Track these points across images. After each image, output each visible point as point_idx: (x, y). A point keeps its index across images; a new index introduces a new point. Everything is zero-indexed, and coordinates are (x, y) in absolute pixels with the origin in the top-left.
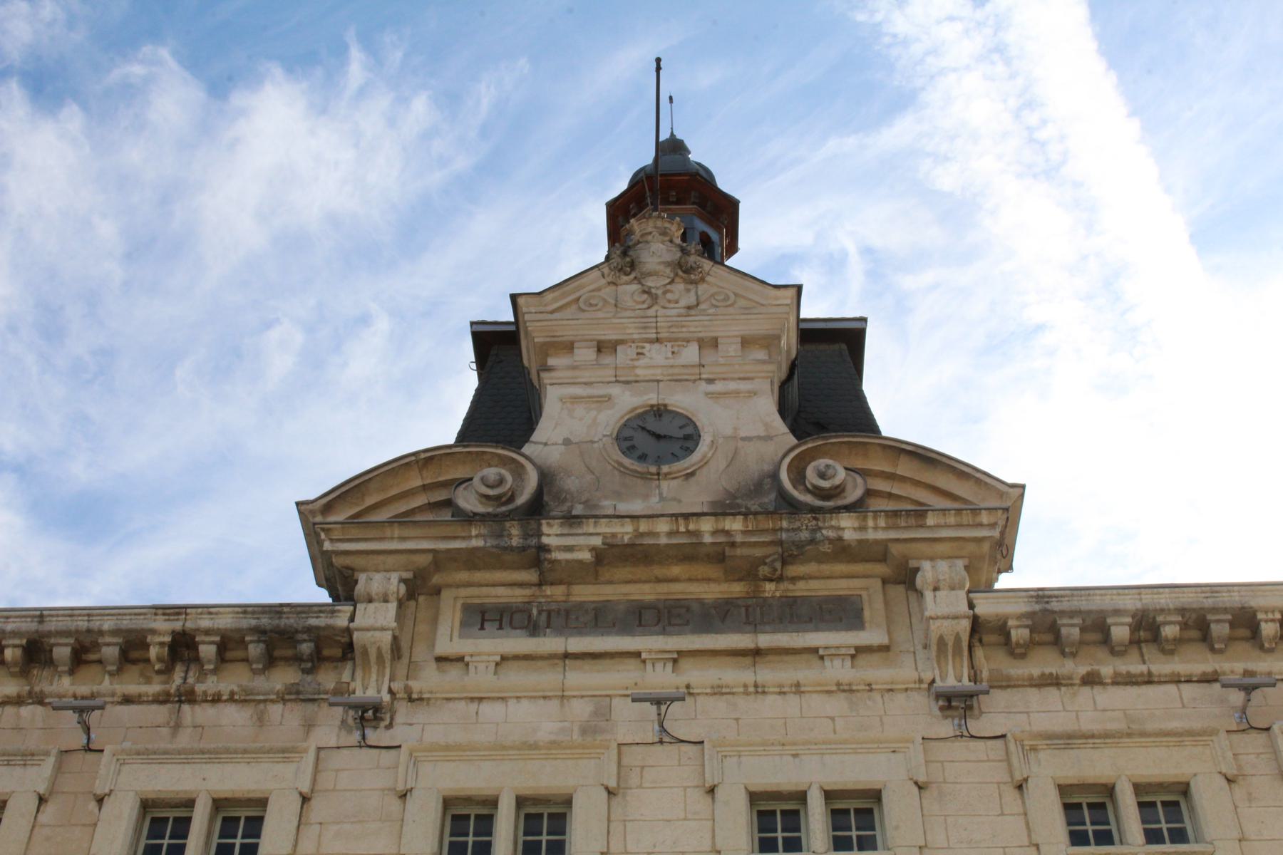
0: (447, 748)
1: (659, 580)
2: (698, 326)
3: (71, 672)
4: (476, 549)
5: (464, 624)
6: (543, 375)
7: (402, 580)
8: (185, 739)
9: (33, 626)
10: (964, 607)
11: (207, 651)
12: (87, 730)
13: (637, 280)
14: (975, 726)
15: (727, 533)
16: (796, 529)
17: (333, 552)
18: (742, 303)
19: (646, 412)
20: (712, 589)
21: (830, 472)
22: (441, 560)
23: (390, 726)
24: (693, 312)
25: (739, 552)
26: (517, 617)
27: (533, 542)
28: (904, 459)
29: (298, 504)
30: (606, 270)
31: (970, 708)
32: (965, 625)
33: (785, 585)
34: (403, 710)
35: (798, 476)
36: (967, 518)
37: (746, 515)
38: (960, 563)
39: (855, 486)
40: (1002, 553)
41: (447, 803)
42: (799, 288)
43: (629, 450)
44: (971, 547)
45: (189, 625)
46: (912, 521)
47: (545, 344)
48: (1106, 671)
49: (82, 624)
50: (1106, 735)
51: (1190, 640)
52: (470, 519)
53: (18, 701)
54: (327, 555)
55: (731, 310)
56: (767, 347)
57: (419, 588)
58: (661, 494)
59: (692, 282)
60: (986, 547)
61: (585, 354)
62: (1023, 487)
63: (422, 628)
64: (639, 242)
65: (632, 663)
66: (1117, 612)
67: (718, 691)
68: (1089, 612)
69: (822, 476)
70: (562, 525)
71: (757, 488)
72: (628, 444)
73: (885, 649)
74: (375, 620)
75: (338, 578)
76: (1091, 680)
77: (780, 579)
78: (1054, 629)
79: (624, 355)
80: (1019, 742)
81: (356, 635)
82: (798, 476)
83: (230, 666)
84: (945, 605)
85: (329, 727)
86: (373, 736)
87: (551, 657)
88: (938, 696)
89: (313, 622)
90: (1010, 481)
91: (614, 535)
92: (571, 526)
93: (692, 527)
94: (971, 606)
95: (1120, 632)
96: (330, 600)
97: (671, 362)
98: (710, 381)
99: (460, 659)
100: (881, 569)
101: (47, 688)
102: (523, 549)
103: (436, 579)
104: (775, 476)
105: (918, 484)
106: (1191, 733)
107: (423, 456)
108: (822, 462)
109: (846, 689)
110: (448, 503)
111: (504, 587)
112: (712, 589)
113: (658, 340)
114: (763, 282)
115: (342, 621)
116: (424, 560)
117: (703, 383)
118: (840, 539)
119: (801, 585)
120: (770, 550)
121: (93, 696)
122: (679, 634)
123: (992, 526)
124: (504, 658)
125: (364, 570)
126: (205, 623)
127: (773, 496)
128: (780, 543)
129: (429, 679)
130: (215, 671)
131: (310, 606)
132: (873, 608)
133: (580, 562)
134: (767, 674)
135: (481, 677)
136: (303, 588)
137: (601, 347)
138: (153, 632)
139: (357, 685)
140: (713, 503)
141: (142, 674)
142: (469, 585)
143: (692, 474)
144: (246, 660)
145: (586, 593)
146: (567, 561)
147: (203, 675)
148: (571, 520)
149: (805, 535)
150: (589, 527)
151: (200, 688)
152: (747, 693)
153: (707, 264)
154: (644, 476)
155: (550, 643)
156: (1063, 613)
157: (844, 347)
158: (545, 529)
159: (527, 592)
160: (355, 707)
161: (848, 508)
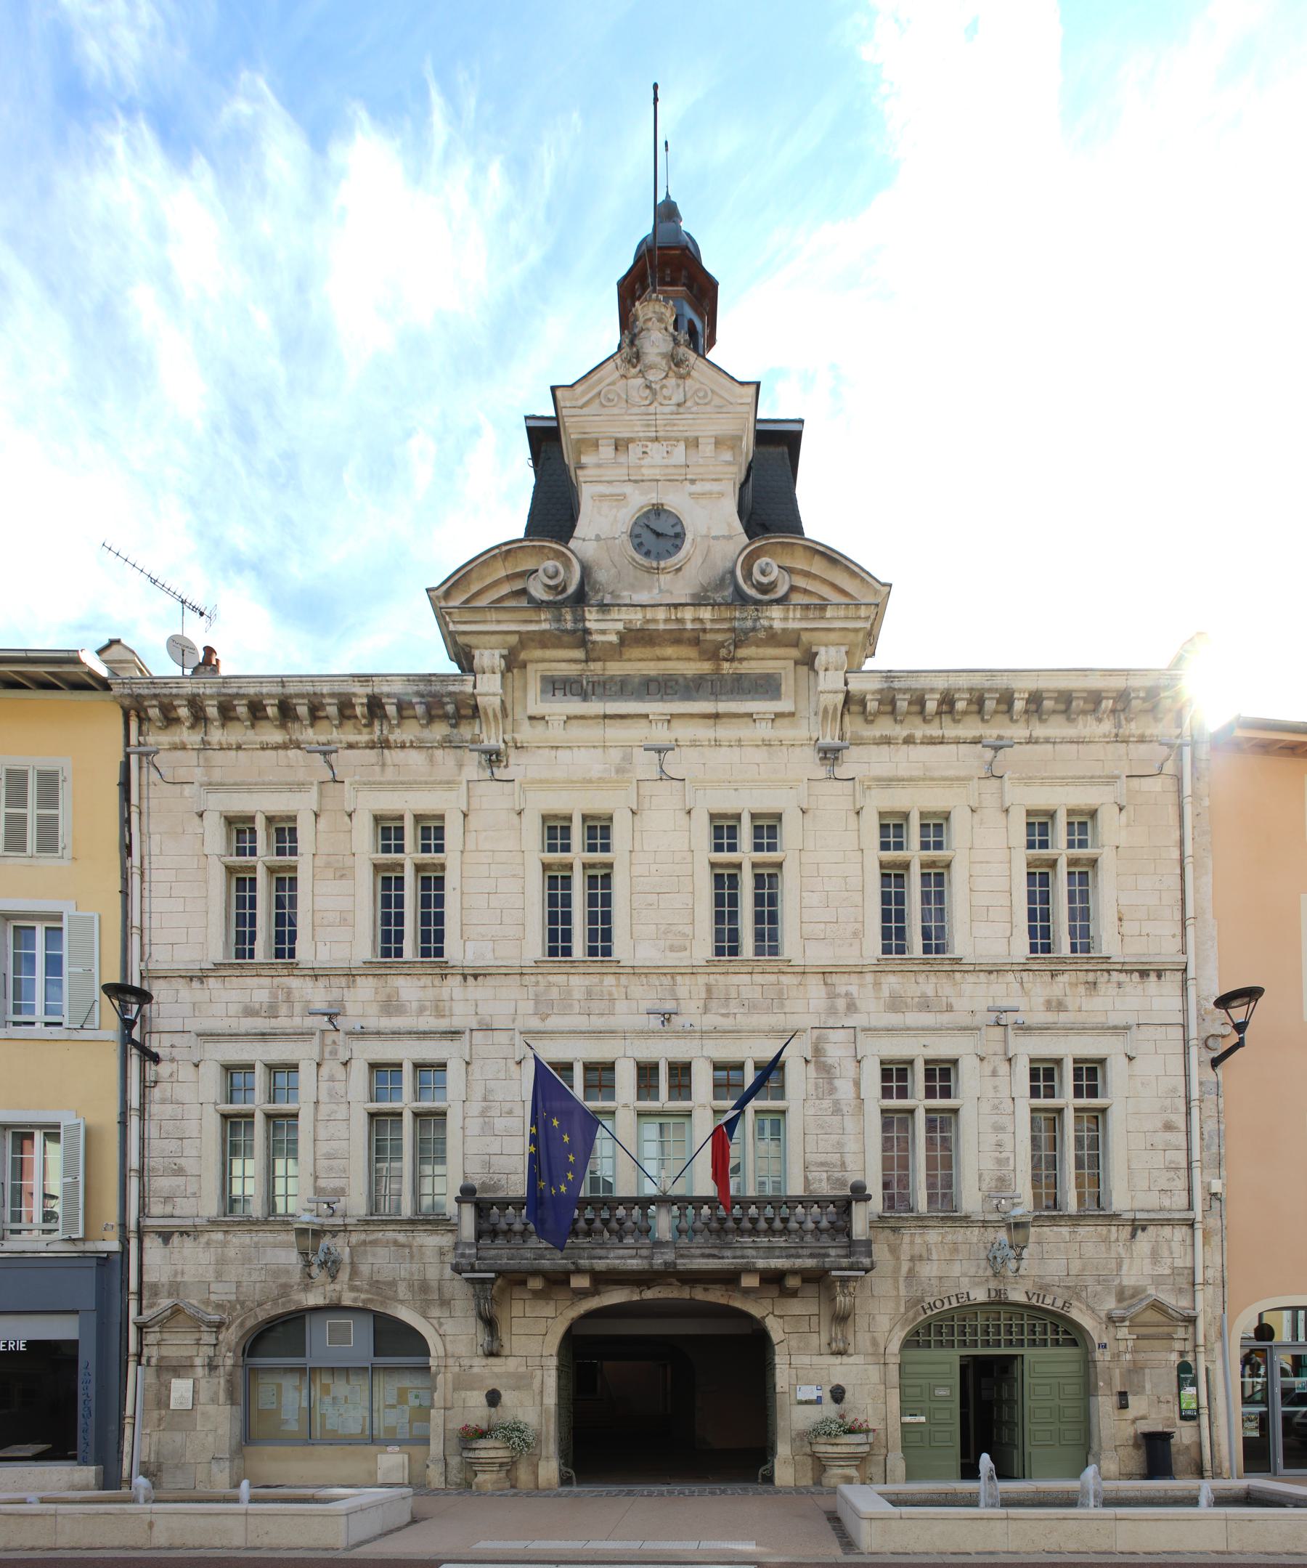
0: (541, 781)
1: (659, 659)
2: (686, 426)
3: (312, 725)
4: (544, 632)
5: (543, 691)
6: (580, 472)
7: (503, 657)
8: (390, 774)
9: (279, 690)
11: (391, 710)
12: (331, 767)
14: (840, 772)
15: (701, 620)
16: (743, 618)
17: (456, 632)
18: (717, 401)
19: (649, 511)
20: (690, 666)
21: (768, 570)
22: (526, 640)
23: (506, 766)
24: (681, 410)
25: (709, 637)
26: (574, 686)
27: (580, 626)
28: (817, 558)
29: (428, 590)
30: (619, 361)
31: (836, 758)
32: (841, 697)
33: (736, 664)
35: (748, 575)
36: (851, 612)
37: (713, 605)
38: (843, 649)
40: (869, 640)
41: (545, 818)
42: (758, 384)
43: (638, 547)
44: (851, 636)
45: (377, 690)
46: (817, 614)
47: (579, 441)
48: (918, 734)
49: (310, 689)
50: (910, 779)
51: (972, 713)
52: (539, 605)
53: (284, 746)
54: (451, 633)
55: (708, 408)
56: (733, 448)
57: (513, 663)
59: (682, 377)
60: (861, 635)
61: (607, 451)
62: (890, 585)
63: (518, 694)
64: (642, 330)
65: (644, 722)
66: (932, 690)
67: (694, 744)
68: (916, 689)
69: (763, 573)
70: (598, 612)
71: (720, 584)
72: (639, 540)
73: (792, 714)
74: (488, 687)
75: (463, 655)
76: (909, 741)
77: (732, 660)
78: (893, 702)
79: (635, 450)
80: (861, 782)
81: (479, 699)
82: (748, 575)
83: (407, 722)
84: (830, 683)
85: (472, 767)
86: (499, 773)
87: (597, 717)
88: (820, 750)
89: (451, 688)
90: (882, 581)
91: (631, 621)
92: (603, 612)
93: (679, 616)
94: (846, 684)
95: (931, 706)
96: (459, 672)
97: (666, 462)
98: (693, 481)
99: (543, 718)
100: (795, 653)
101: (301, 738)
102: (574, 631)
103: (523, 656)
104: (732, 572)
105: (824, 581)
106: (958, 779)
107: (504, 548)
108: (763, 560)
109: (767, 744)
110: (524, 592)
111: (564, 662)
112: (690, 666)
113: (656, 439)
114: (732, 378)
115: (469, 689)
116: (514, 640)
117: (687, 483)
118: (771, 627)
119: (745, 664)
120: (728, 635)
121: (329, 743)
123: (867, 618)
124: (568, 718)
125: (477, 648)
126: (386, 689)
127: (731, 589)
128: (733, 630)
129: (526, 733)
130: (399, 725)
131: (448, 676)
132: (787, 686)
133: (610, 643)
134: (726, 732)
135: (556, 732)
136: (441, 663)
137: (620, 445)
138: (355, 695)
139: (484, 736)
140: (693, 596)
141: (355, 728)
142: (543, 661)
143: (679, 570)
144: (415, 717)
145: (615, 668)
146: (603, 642)
147: (391, 727)
148: (604, 607)
149: (749, 624)
150: (614, 614)
151: (392, 738)
152: (710, 746)
153: (692, 356)
154: (649, 570)
155: (595, 707)
156: (900, 689)
157: (786, 449)
158: (588, 616)
159: (579, 667)
160: (485, 752)
161: (778, 601)
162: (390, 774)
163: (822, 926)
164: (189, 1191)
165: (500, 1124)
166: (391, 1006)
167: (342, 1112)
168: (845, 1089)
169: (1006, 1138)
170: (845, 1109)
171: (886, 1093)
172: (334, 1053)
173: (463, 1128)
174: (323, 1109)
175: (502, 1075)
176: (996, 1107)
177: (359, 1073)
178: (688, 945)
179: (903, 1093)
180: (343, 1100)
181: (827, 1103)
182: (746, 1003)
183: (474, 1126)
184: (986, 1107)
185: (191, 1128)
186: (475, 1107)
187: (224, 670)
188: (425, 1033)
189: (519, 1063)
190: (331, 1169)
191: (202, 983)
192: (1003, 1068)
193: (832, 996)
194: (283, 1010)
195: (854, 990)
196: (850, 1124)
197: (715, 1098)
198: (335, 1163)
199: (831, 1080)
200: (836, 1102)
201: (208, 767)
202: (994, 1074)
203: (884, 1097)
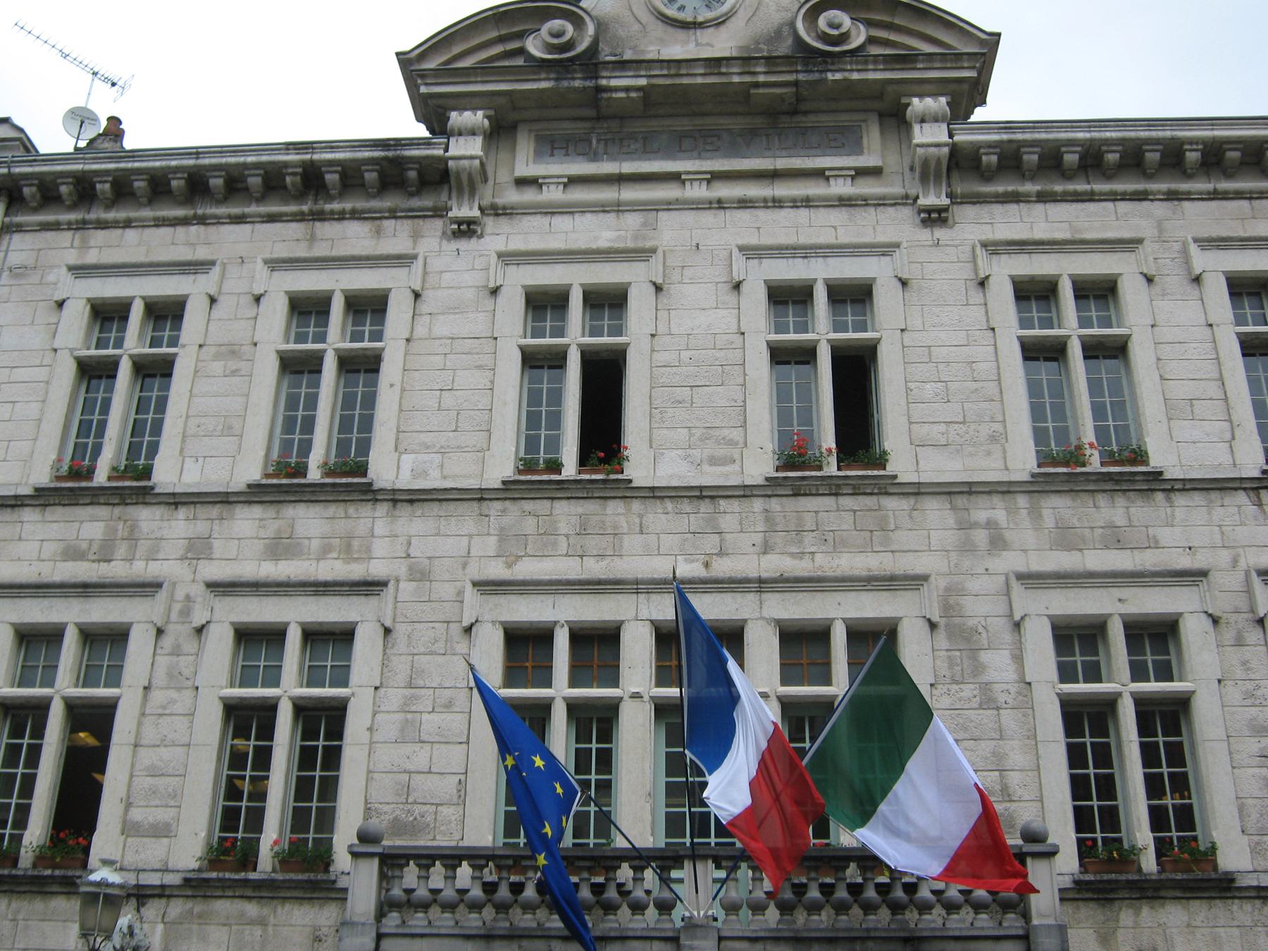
10: (944, 138)
29: (398, 54)
34: (489, 222)
39: (859, 35)
40: (976, 92)
44: (953, 87)
58: (696, 40)
60: (966, 87)
62: (999, 35)
81: (451, 163)
88: (920, 211)
94: (951, 136)
96: (427, 134)
104: (792, 24)
109: (844, 202)
122: (712, 158)
125: (454, 109)
127: (790, 41)
136: (403, 123)
159: (588, 125)
163: (942, 428)
165: (430, 722)
166: (279, 548)
168: (998, 665)
170: (1002, 698)
171: (1066, 673)
172: (186, 613)
173: (370, 729)
174: (157, 696)
175: (440, 646)
177: (221, 643)
178: (737, 456)
179: (1094, 674)
180: (189, 683)
181: (968, 690)
182: (830, 537)
183: (389, 725)
184: (1234, 693)
186: (394, 697)
187: (129, 143)
188: (326, 584)
189: (468, 630)
190: (154, 792)
193: (965, 526)
194: (122, 550)
195: (1000, 515)
196: (1009, 719)
197: (784, 682)
198: (161, 782)
199: (974, 652)
200: (986, 687)
203: (1063, 679)
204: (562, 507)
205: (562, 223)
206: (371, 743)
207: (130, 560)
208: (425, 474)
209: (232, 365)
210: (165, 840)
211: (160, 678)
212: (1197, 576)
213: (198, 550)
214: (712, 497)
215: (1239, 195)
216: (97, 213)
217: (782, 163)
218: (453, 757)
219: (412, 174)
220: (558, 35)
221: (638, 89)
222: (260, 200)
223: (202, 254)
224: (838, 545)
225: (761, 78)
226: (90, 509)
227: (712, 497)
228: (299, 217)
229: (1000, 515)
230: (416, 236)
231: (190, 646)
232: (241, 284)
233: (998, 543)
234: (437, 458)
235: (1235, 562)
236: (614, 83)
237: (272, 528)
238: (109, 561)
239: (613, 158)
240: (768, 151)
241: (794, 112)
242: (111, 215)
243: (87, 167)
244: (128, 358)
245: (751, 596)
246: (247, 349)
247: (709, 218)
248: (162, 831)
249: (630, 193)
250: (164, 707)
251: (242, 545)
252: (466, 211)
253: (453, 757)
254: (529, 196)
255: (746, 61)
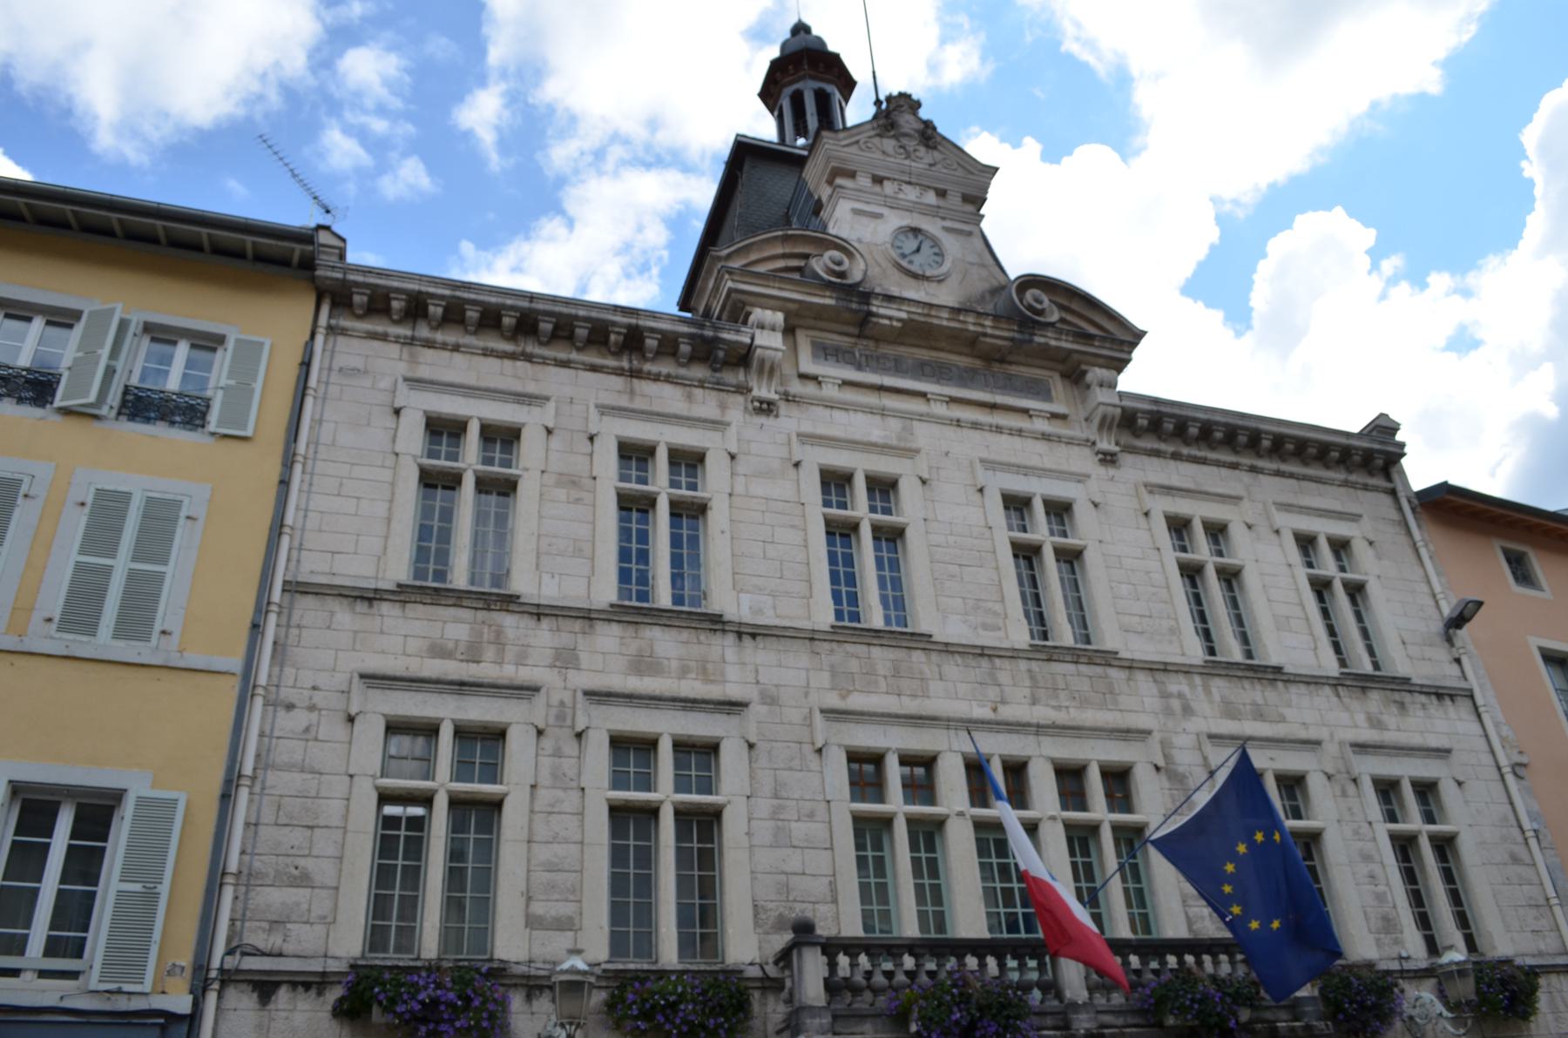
13: (896, 137)
34: (783, 408)
79: (889, 188)
109: (1046, 437)
159: (852, 340)
162: (639, 404)
163: (1137, 619)
164: (316, 912)
165: (799, 830)
166: (644, 664)
167: (571, 800)
169: (1377, 869)
175: (796, 763)
176: (1356, 832)
183: (764, 831)
185: (332, 810)
186: (764, 806)
190: (552, 886)
191: (371, 606)
192: (1351, 788)
193: (1165, 695)
194: (490, 653)
195: (1185, 689)
198: (559, 877)
201: (413, 361)
202: (1344, 794)
204: (876, 652)
205: (838, 415)
206: (751, 846)
207: (501, 663)
208: (760, 611)
209: (575, 494)
210: (570, 934)
211: (545, 778)
212: (1313, 744)
213: (565, 660)
214: (989, 656)
215: (1291, 476)
216: (423, 331)
217: (1000, 399)
218: (819, 862)
219: (721, 354)
220: (839, 263)
221: (899, 320)
222: (617, 354)
223: (531, 388)
224: (1084, 703)
225: (989, 331)
226: (452, 610)
227: (989, 656)
228: (618, 372)
229: (1185, 689)
230: (723, 407)
231: (571, 747)
232: (572, 423)
233: (1187, 710)
234: (769, 600)
235: (1332, 735)
236: (882, 311)
237: (633, 646)
238: (478, 662)
239: (875, 371)
240: (985, 387)
241: (1002, 361)
242: (439, 336)
243: (424, 289)
244: (465, 468)
245: (1032, 738)
246: (589, 482)
247: (951, 432)
248: (564, 924)
249: (890, 402)
250: (552, 806)
251: (607, 656)
252: (763, 391)
253: (819, 862)
254: (809, 389)
255: (956, 311)
